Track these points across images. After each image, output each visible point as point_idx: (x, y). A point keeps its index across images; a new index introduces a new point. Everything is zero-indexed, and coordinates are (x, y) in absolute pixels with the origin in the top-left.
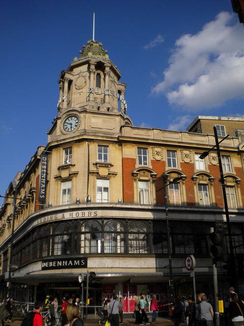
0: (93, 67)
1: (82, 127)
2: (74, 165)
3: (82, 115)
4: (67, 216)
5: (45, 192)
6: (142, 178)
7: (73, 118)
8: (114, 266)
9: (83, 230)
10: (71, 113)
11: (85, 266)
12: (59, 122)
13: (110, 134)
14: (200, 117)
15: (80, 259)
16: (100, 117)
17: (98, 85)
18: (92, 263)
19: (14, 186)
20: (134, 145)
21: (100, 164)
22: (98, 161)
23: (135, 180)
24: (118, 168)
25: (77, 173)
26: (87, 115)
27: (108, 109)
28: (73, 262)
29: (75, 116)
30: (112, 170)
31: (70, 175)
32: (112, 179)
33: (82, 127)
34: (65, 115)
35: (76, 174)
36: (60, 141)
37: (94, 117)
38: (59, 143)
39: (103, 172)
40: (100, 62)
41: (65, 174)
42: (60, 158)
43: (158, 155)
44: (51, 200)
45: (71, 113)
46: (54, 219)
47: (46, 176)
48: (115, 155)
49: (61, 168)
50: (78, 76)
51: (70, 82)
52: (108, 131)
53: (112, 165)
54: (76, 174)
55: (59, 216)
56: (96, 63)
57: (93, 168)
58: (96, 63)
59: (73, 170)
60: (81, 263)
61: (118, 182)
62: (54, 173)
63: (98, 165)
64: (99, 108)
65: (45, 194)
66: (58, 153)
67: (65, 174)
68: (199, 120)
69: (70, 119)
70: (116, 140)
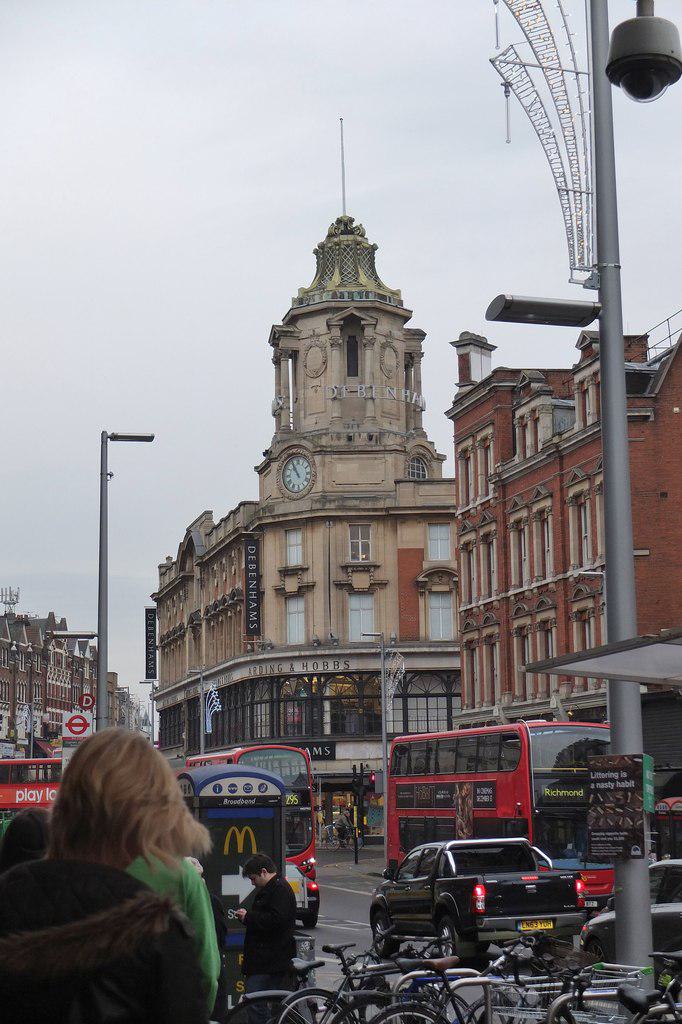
0: (336, 332)
1: (318, 487)
2: (307, 569)
3: (318, 458)
4: (298, 668)
5: (258, 616)
6: (434, 589)
9: (327, 694)
10: (294, 451)
11: (332, 757)
12: (274, 466)
13: (375, 499)
15: (322, 745)
16: (353, 459)
17: (353, 368)
18: (343, 751)
19: (199, 551)
20: (421, 520)
21: (353, 566)
22: (349, 560)
23: (422, 594)
24: (389, 572)
26: (328, 458)
27: (370, 438)
30: (380, 575)
32: (380, 593)
33: (318, 487)
34: (284, 457)
35: (311, 587)
36: (279, 516)
37: (341, 459)
38: (277, 520)
39: (361, 581)
41: (291, 585)
42: (284, 548)
44: (270, 634)
45: (294, 451)
47: (258, 585)
48: (383, 547)
49: (286, 572)
50: (308, 341)
51: (294, 355)
52: (370, 488)
53: (377, 567)
54: (311, 587)
55: (286, 668)
56: (342, 322)
57: (342, 577)
59: (307, 578)
61: (390, 597)
62: (270, 580)
63: (350, 570)
64: (350, 439)
65: (258, 622)
67: (291, 585)
70: (384, 513)
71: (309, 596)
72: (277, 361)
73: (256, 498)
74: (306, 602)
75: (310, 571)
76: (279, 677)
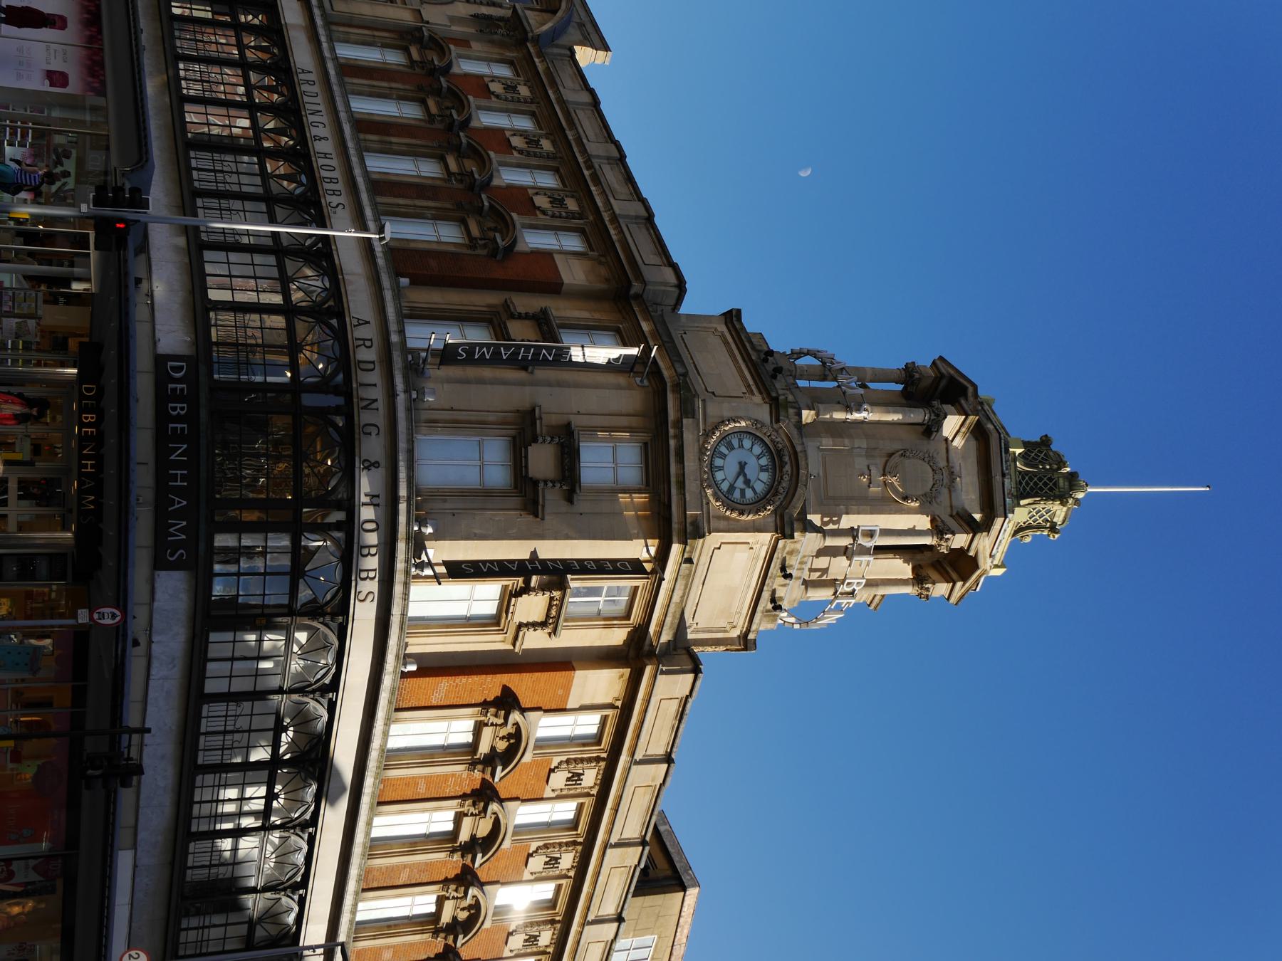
7: (765, 476)
8: (155, 664)
10: (788, 468)
11: (159, 563)
14: (692, 893)
25: (537, 516)
28: (179, 514)
29: (772, 490)
31: (535, 483)
38: (671, 431)
40: (977, 567)
43: (569, 779)
46: (365, 417)
55: (372, 447)
56: (972, 553)
58: (972, 553)
59: (552, 497)
60: (177, 545)
66: (634, 421)
67: (542, 460)
68: (684, 889)
69: (764, 461)
71: (515, 501)
72: (909, 374)
73: (685, 309)
74: (502, 494)
75: (564, 507)
76: (350, 418)
